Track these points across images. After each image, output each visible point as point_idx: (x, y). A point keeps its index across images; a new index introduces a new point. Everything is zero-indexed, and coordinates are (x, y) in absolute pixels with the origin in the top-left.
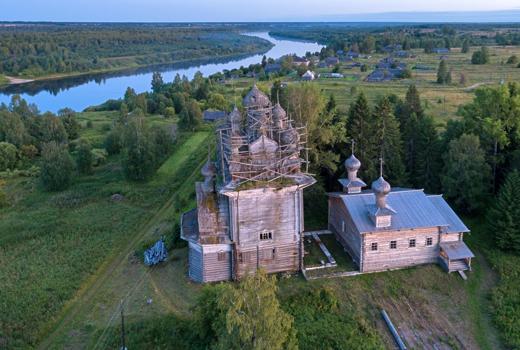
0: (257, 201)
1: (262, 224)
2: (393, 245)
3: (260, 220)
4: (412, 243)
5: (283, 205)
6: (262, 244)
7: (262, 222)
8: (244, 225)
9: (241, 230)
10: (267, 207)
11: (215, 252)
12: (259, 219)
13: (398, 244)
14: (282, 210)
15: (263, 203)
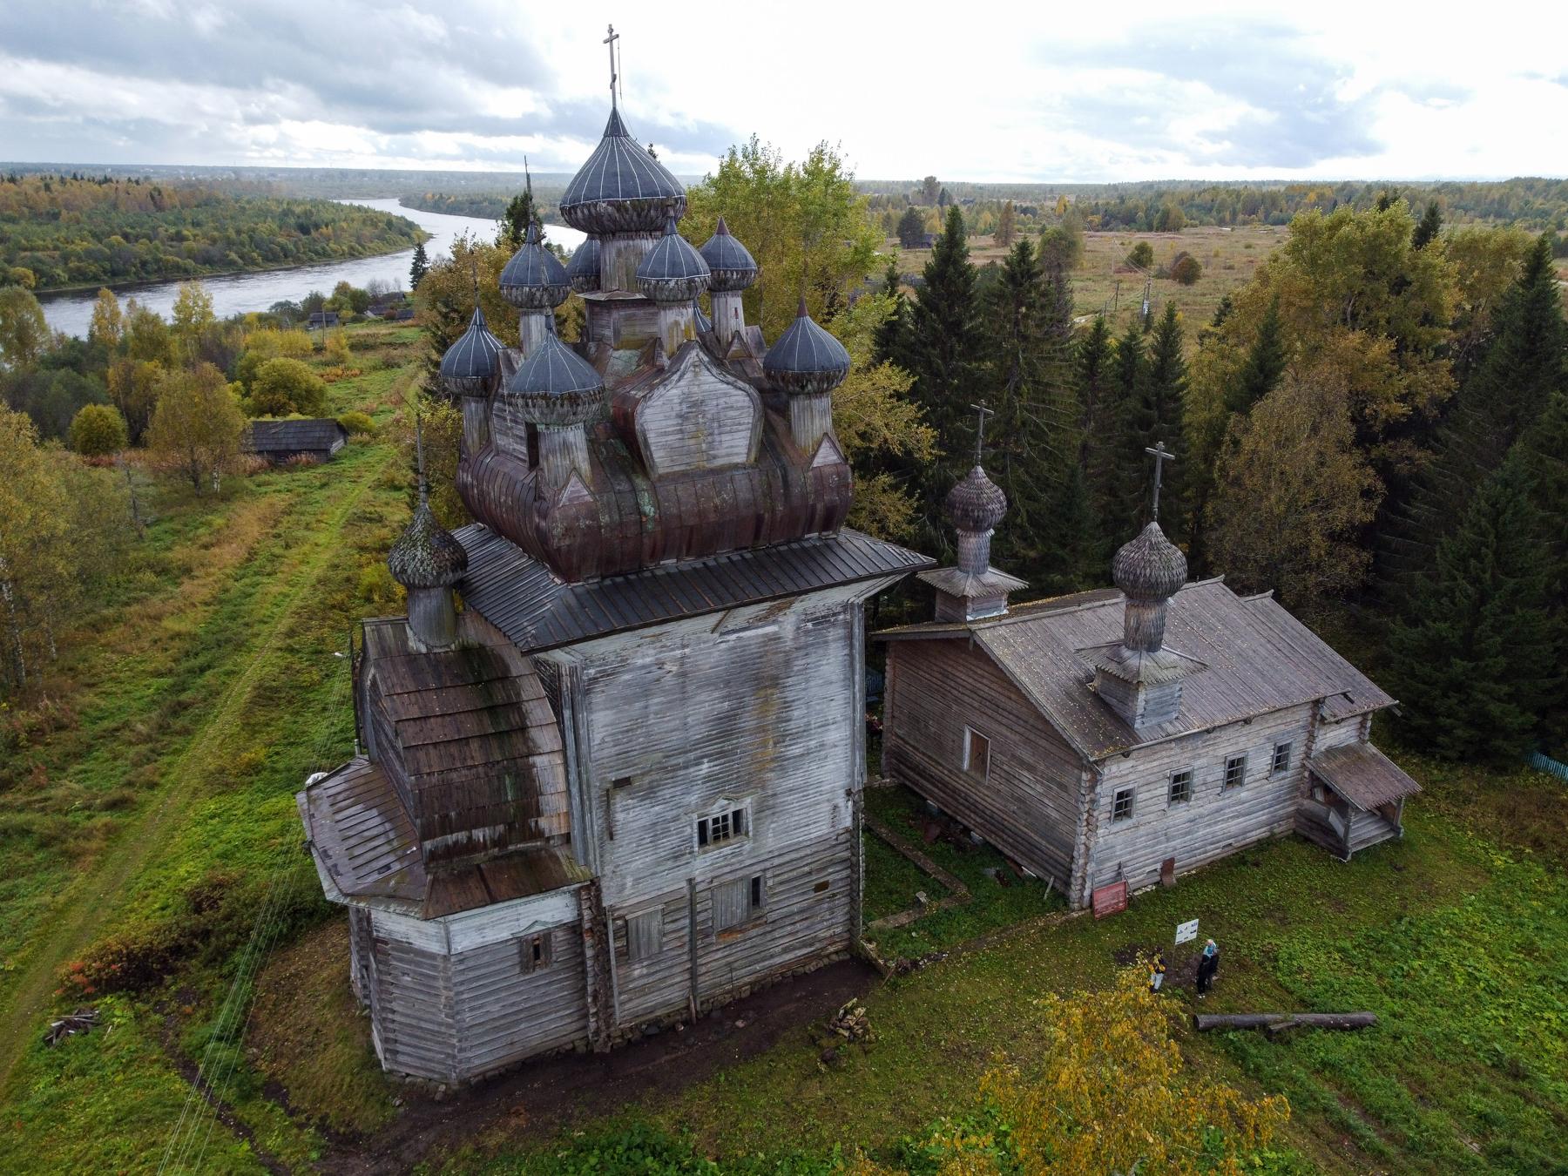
0: (683, 675)
1: (709, 778)
3: (698, 762)
5: (790, 681)
8: (631, 795)
9: (620, 816)
10: (724, 698)
12: (692, 756)
14: (787, 705)
15: (709, 683)
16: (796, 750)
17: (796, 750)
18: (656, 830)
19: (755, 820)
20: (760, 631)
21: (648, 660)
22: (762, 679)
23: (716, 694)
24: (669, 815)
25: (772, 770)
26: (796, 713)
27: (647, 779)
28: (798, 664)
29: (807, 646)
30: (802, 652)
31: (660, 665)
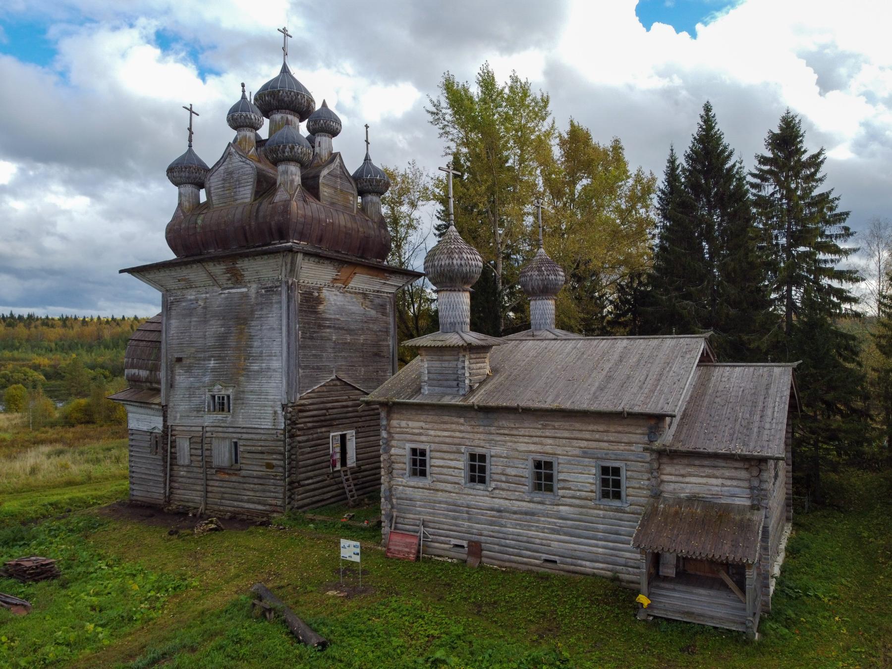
0: (205, 308)
1: (214, 370)
2: (478, 470)
4: (544, 476)
5: (253, 323)
6: (210, 419)
7: (212, 364)
9: (177, 377)
10: (222, 326)
11: (145, 428)
12: (207, 354)
13: (493, 467)
14: (251, 338)
16: (255, 367)
17: (255, 367)
19: (234, 404)
20: (239, 290)
21: (193, 297)
22: (240, 318)
23: (219, 322)
24: (197, 385)
25: (243, 376)
27: (188, 361)
28: (257, 314)
29: (262, 304)
30: (260, 307)
31: (197, 300)
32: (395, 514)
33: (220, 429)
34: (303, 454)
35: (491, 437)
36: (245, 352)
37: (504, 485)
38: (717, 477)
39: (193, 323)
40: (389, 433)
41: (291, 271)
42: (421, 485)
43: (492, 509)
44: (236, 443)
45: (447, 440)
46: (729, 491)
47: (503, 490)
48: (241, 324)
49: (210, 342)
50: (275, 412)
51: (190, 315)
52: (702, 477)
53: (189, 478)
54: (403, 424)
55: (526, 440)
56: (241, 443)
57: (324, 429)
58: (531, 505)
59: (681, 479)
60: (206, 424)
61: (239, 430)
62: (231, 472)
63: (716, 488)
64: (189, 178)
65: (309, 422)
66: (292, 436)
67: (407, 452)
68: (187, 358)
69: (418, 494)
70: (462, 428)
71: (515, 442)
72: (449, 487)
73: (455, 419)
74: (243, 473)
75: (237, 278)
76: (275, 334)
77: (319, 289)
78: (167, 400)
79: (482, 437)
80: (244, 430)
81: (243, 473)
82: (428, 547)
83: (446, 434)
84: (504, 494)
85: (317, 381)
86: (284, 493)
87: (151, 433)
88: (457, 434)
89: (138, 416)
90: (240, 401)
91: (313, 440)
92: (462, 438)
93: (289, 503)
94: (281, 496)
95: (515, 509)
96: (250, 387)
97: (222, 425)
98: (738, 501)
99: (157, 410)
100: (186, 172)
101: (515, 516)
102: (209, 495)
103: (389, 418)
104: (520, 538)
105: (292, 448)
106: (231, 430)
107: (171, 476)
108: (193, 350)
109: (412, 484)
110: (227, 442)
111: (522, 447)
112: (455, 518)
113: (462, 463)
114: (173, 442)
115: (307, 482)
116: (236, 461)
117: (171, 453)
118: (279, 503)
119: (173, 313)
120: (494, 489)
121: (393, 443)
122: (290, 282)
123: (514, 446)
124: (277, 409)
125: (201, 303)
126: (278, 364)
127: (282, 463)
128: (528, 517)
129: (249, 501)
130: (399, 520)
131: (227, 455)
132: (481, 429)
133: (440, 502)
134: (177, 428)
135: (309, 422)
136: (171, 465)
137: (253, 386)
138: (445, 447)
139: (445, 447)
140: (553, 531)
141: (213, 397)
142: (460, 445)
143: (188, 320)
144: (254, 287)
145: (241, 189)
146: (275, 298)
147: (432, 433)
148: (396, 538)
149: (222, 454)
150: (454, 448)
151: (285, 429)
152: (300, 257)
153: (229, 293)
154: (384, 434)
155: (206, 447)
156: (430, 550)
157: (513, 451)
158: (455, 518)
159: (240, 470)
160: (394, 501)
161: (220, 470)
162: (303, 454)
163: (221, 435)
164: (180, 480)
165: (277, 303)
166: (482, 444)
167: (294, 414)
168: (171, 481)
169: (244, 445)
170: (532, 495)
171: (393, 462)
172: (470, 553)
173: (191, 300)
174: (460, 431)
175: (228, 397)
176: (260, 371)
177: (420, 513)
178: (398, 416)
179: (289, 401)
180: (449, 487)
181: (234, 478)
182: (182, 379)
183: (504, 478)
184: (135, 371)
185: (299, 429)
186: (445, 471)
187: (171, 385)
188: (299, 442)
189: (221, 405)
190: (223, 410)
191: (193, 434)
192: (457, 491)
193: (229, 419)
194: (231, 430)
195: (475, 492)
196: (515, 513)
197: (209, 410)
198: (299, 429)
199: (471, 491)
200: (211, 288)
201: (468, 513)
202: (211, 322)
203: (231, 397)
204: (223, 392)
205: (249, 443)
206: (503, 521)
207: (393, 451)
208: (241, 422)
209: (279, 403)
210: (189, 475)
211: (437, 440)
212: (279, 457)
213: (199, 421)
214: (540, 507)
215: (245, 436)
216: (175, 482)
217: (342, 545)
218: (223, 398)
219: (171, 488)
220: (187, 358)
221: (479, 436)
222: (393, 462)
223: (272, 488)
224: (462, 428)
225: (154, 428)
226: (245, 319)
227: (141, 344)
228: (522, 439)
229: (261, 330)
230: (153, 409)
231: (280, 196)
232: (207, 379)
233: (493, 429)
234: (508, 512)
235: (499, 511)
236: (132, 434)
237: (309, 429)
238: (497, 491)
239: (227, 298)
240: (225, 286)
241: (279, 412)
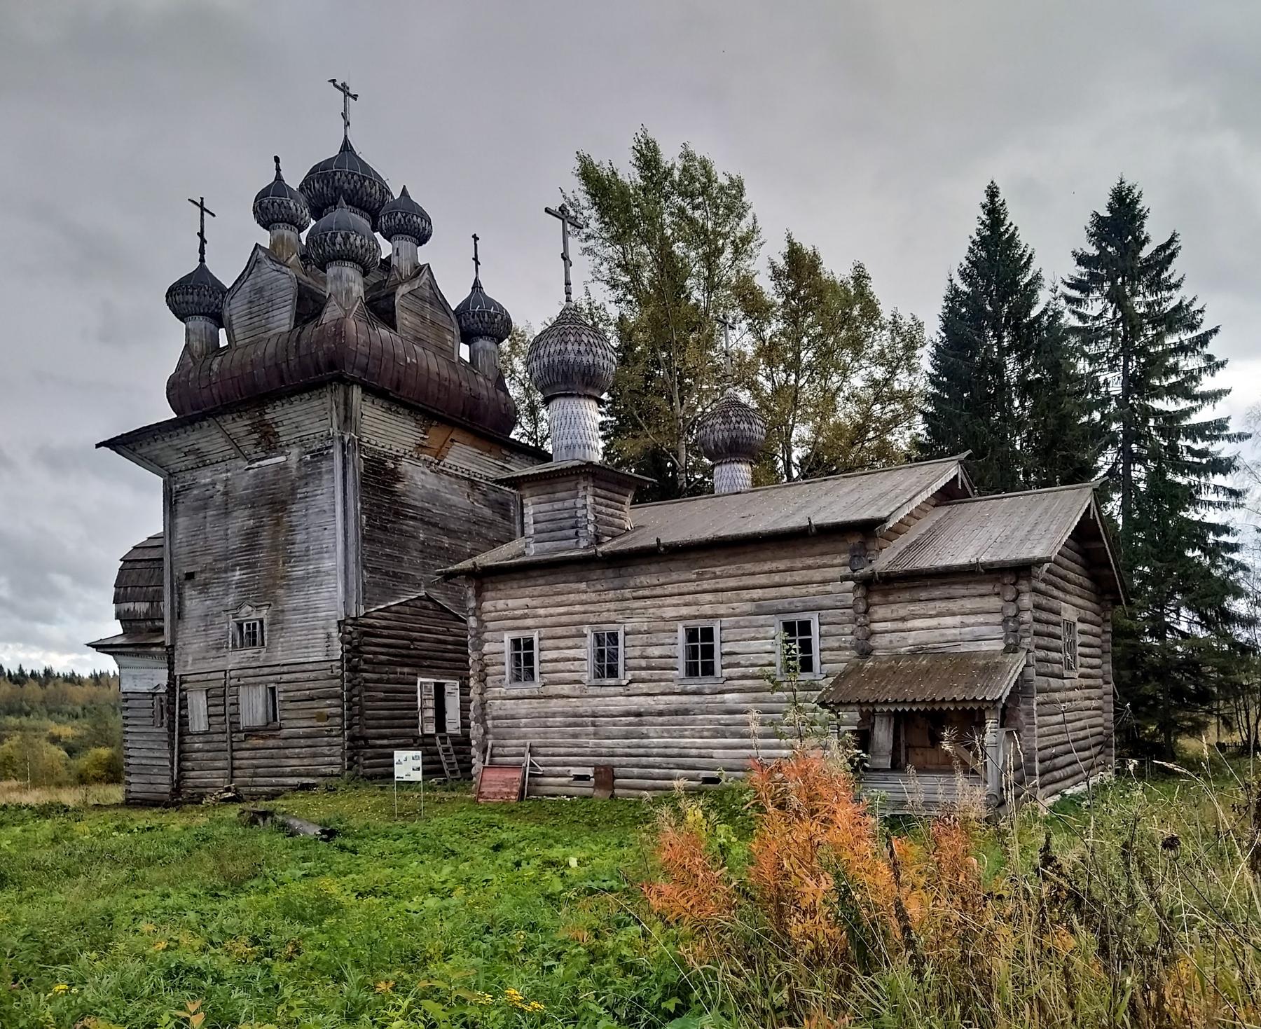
0: (226, 494)
1: (240, 584)
5: (295, 507)
8: (194, 587)
9: (188, 603)
10: (251, 517)
11: (145, 689)
14: (292, 529)
16: (299, 572)
17: (299, 572)
18: (208, 620)
19: (270, 631)
22: (275, 502)
23: (247, 512)
25: (281, 587)
26: (299, 537)
29: (306, 476)
30: (304, 481)
31: (214, 484)
32: (490, 743)
33: (251, 672)
34: (372, 699)
35: (626, 604)
36: (284, 552)
37: (644, 674)
38: (953, 614)
39: (209, 519)
40: (481, 622)
41: (346, 417)
42: (526, 692)
43: (627, 714)
44: (273, 689)
45: (564, 619)
46: (972, 632)
47: (643, 681)
48: (277, 511)
49: (235, 543)
50: (329, 636)
51: (205, 507)
52: (931, 616)
53: (208, 751)
54: (501, 604)
55: (675, 600)
56: (280, 688)
57: (406, 670)
58: (684, 698)
59: (900, 625)
60: (230, 667)
61: (277, 669)
62: (267, 734)
63: (953, 631)
64: (199, 304)
65: (382, 654)
66: (354, 670)
67: (507, 646)
68: (201, 572)
69: (523, 707)
70: (584, 597)
71: (660, 607)
72: (566, 689)
73: (574, 586)
74: (285, 732)
75: (269, 441)
76: (327, 518)
77: (396, 459)
78: (173, 638)
79: (612, 606)
80: (285, 669)
81: (285, 732)
82: (538, 785)
83: (562, 610)
84: (644, 687)
85: (394, 595)
86: (342, 755)
87: (154, 694)
88: (578, 608)
89: (134, 672)
90: (279, 626)
91: (388, 681)
92: (584, 613)
93: (350, 768)
94: (339, 760)
95: (661, 707)
96: (293, 603)
97: (254, 664)
98: (985, 646)
99: (161, 655)
100: (194, 297)
101: (660, 719)
102: (237, 772)
103: (479, 596)
104: (668, 751)
105: (354, 686)
106: (266, 670)
107: (181, 752)
108: (210, 559)
109: (514, 693)
110: (261, 689)
111: (670, 613)
112: (575, 736)
113: (587, 650)
114: (184, 700)
115: (379, 742)
116: (275, 719)
117: (180, 716)
118: (336, 770)
119: (180, 507)
120: (631, 682)
121: (487, 635)
122: (346, 439)
123: (658, 612)
124: (331, 630)
125: (220, 487)
126: (333, 563)
127: (339, 709)
128: (680, 718)
129: (292, 775)
130: (496, 751)
131: (261, 710)
132: (611, 594)
133: (554, 715)
134: (189, 678)
135: (382, 654)
136: (180, 735)
137: (297, 601)
138: (560, 631)
139: (560, 631)
140: (717, 734)
141: (240, 626)
142: (582, 623)
143: (201, 515)
144: (295, 452)
145: (275, 313)
146: (325, 466)
147: (542, 611)
148: (491, 775)
149: (253, 708)
150: (573, 630)
151: (341, 659)
152: (357, 393)
153: (260, 466)
154: (472, 622)
155: (229, 700)
156: (541, 788)
157: (655, 618)
158: (575, 736)
159: (281, 728)
160: (489, 723)
161: (252, 732)
162: (372, 699)
163: (252, 680)
164: (194, 755)
165: (327, 472)
166: (612, 619)
167: (357, 637)
168: (180, 760)
169: (286, 691)
170: (685, 682)
171: (487, 665)
172: (598, 785)
173: (205, 485)
174: (581, 603)
175: (261, 622)
176: (306, 578)
177: (525, 736)
178: (493, 594)
179: (347, 616)
180: (566, 689)
181: (271, 743)
182: (194, 604)
183: (643, 663)
184: (131, 605)
185: (366, 662)
186: (560, 666)
187: (178, 615)
188: (366, 681)
189: (250, 636)
190: (254, 644)
191: (212, 684)
192: (577, 693)
193: (263, 655)
194: (266, 670)
195: (603, 691)
196: (660, 714)
197: (234, 646)
198: (366, 662)
199: (598, 691)
200: (233, 464)
201: (594, 725)
202: (235, 514)
203: (265, 621)
204: (253, 617)
205: (292, 686)
206: (644, 729)
207: (487, 648)
208: (280, 656)
209: (335, 621)
210: (207, 747)
211: (549, 621)
212: (334, 702)
213: (219, 664)
214: (696, 698)
215: (285, 677)
216: (187, 760)
217: (396, 760)
218: (254, 625)
219: (181, 770)
220: (201, 572)
221: (608, 605)
222: (487, 665)
223: (326, 750)
224: (584, 597)
225: (157, 687)
226: (284, 502)
227: (138, 565)
228: (669, 601)
229: (305, 516)
230: (153, 655)
231: (330, 314)
232: (231, 600)
233: (627, 593)
234: (651, 714)
235: (639, 715)
236: (127, 700)
237: (381, 663)
238: (635, 685)
239: (256, 475)
240: (254, 456)
241: (334, 635)
